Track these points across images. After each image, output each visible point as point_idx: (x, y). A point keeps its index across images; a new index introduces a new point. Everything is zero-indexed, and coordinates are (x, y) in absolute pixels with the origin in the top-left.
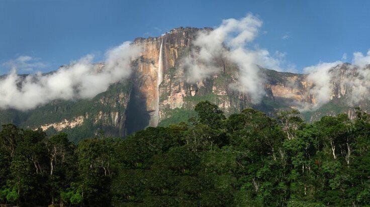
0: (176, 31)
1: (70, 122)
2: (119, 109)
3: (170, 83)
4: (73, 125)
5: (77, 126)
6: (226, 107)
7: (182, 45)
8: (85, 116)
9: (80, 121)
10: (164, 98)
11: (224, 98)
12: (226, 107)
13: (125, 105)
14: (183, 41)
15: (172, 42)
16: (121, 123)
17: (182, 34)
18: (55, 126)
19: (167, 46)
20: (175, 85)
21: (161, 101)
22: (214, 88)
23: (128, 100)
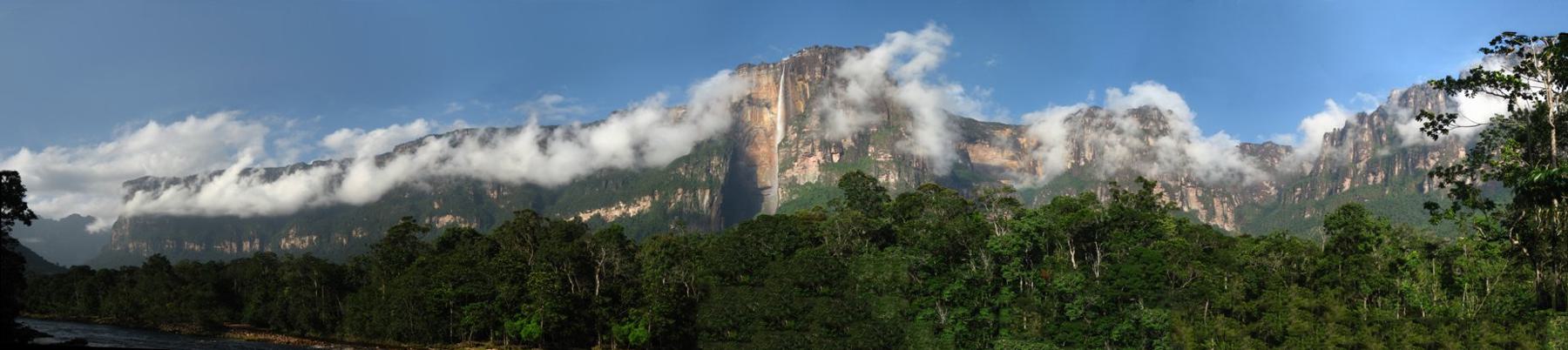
0: (806, 53)
1: (628, 206)
2: (711, 184)
3: (797, 140)
4: (633, 211)
5: (640, 213)
6: (892, 180)
7: (818, 75)
8: (653, 195)
9: (645, 204)
10: (786, 165)
11: (888, 165)
12: (892, 180)
13: (721, 178)
14: (818, 69)
15: (801, 71)
16: (715, 207)
17: (816, 57)
18: (602, 212)
19: (792, 78)
20: (806, 144)
21: (782, 170)
22: (871, 149)
23: (725, 169)
